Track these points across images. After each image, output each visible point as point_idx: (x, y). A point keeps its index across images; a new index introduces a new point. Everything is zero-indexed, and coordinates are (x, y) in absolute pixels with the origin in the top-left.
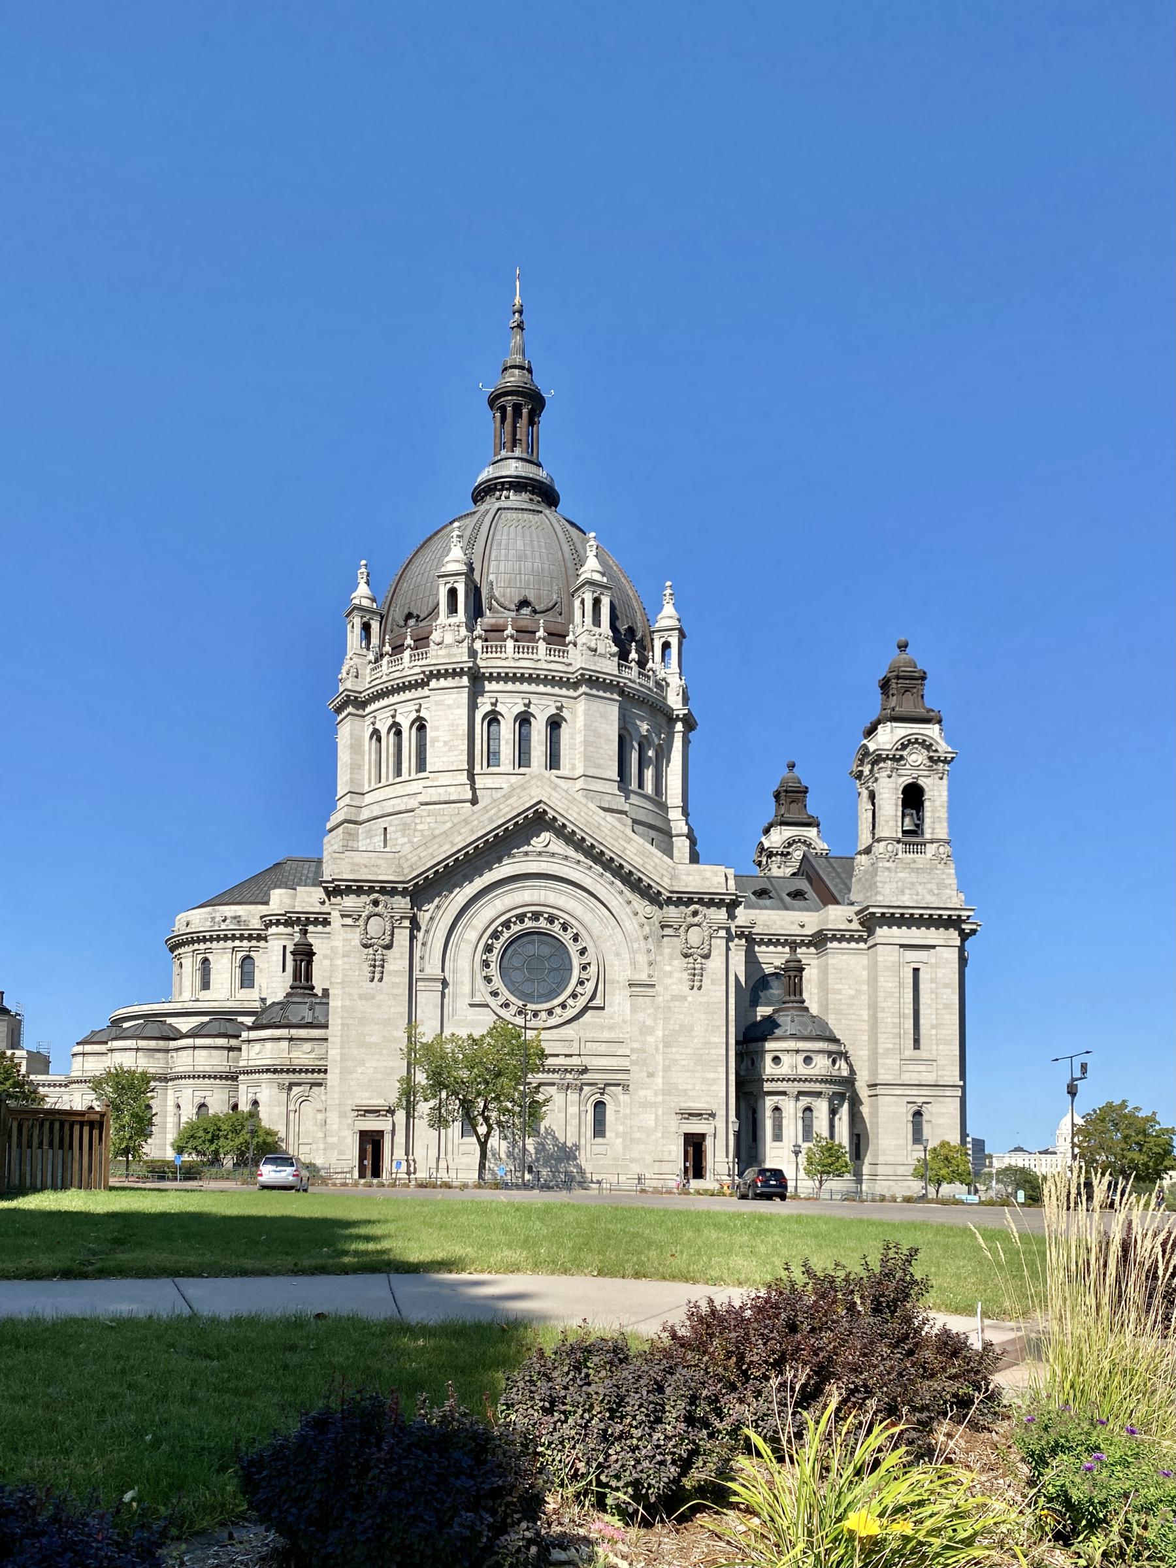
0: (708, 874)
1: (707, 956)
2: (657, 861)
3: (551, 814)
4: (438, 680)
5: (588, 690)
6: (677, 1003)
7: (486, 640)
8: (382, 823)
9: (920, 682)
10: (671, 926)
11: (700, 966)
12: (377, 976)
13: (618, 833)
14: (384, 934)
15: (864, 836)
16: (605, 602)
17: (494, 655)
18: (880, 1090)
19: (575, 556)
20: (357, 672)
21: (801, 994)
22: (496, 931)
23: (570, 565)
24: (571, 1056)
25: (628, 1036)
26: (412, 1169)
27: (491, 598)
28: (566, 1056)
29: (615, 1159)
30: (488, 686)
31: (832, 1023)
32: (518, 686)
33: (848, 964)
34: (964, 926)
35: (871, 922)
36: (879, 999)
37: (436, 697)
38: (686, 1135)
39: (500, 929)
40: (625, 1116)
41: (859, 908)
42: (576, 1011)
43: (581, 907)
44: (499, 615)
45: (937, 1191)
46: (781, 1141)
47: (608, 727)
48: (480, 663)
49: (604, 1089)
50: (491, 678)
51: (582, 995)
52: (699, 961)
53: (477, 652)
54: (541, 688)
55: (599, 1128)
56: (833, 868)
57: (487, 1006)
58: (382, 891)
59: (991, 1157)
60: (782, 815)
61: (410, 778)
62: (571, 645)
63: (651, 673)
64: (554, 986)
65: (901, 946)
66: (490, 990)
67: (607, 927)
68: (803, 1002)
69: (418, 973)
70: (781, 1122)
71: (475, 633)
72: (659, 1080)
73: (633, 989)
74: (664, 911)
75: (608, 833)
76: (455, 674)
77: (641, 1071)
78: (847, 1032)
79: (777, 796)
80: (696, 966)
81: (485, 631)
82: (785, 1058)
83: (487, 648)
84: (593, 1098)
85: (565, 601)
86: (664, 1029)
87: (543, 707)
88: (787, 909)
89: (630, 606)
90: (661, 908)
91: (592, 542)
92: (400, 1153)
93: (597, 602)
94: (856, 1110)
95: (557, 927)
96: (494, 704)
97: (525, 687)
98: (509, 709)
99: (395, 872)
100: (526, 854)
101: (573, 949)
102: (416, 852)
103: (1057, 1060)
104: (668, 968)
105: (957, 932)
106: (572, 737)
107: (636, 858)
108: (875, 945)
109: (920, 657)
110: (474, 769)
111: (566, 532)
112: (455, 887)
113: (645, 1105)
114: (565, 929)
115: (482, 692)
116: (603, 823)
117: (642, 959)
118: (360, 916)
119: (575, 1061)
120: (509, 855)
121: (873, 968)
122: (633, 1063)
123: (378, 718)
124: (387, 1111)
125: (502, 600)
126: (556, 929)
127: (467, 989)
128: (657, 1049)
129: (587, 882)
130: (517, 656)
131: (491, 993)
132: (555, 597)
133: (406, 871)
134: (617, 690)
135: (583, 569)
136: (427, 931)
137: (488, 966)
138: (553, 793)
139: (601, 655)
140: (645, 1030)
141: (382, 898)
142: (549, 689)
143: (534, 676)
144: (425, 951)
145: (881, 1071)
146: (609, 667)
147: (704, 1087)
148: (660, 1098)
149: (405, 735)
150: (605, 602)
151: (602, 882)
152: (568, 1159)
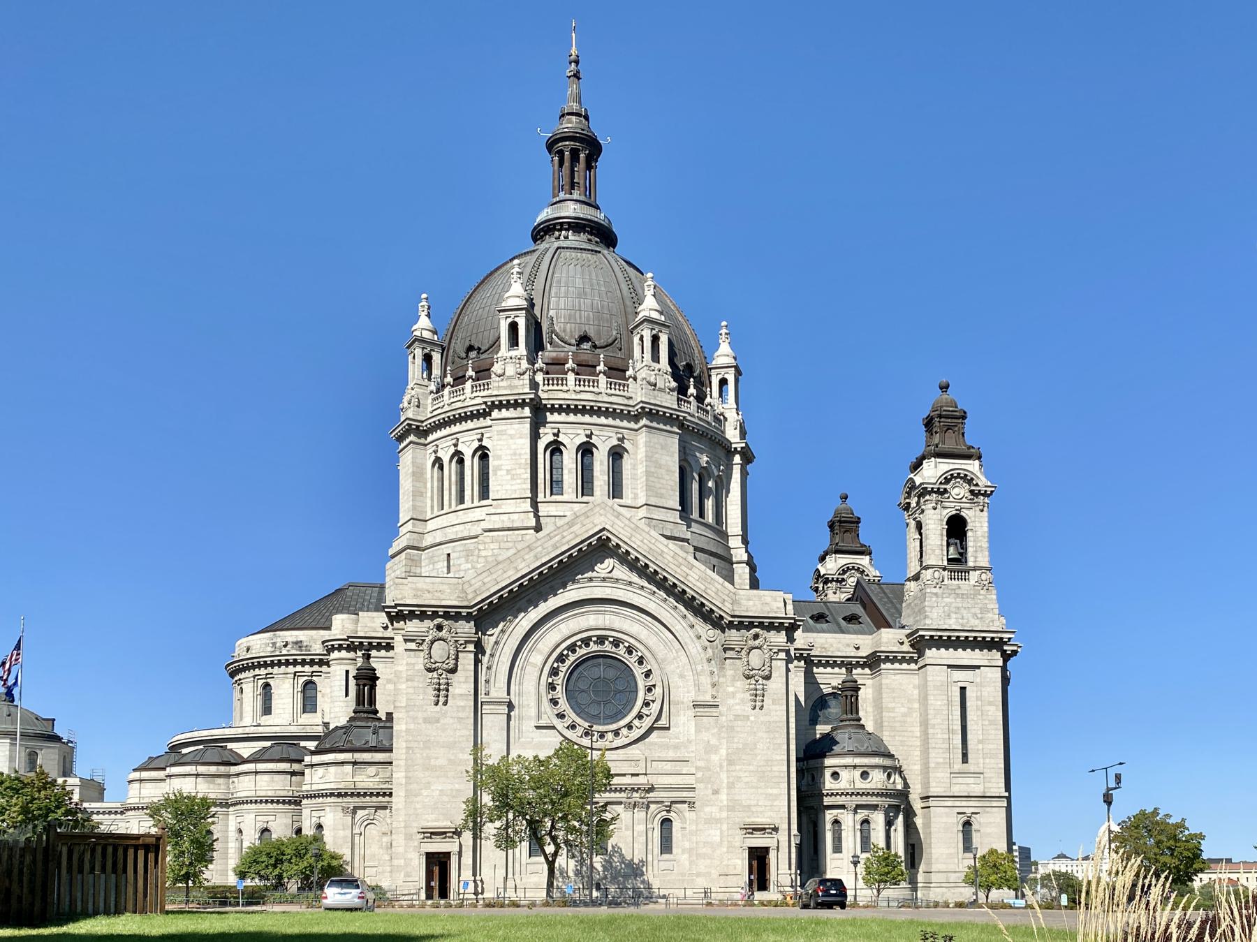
1: (768, 678)
3: (614, 541)
4: (500, 410)
5: (648, 423)
7: (547, 373)
8: (446, 549)
10: (733, 649)
11: (761, 686)
12: (442, 700)
14: (448, 658)
15: (913, 564)
16: (664, 339)
17: (555, 387)
18: (931, 802)
19: (634, 295)
21: (857, 713)
22: (561, 654)
23: (629, 303)
24: (637, 775)
25: (693, 755)
26: (480, 890)
27: (552, 332)
28: (633, 775)
29: (683, 875)
30: (550, 417)
31: (886, 740)
32: (579, 418)
33: (901, 684)
34: (1005, 648)
35: (920, 644)
36: (930, 717)
37: (498, 427)
38: (751, 849)
39: (565, 652)
41: (909, 631)
42: (642, 731)
44: (560, 349)
45: (987, 897)
47: (668, 458)
48: (542, 395)
49: (670, 806)
50: (553, 410)
51: (647, 716)
52: (760, 682)
53: (538, 384)
54: (603, 420)
55: (666, 845)
56: (885, 593)
57: (554, 728)
58: (447, 616)
59: (1036, 863)
60: (837, 544)
61: (473, 506)
62: (631, 380)
63: (709, 408)
64: (620, 707)
65: (949, 666)
66: (556, 713)
67: (672, 651)
68: (859, 720)
69: (483, 696)
70: (841, 834)
71: (536, 365)
72: (723, 797)
74: (726, 634)
76: (516, 405)
77: (706, 788)
78: (901, 748)
79: (831, 526)
80: (758, 687)
81: (547, 364)
82: (844, 774)
83: (548, 381)
84: (659, 816)
85: (624, 338)
86: (728, 748)
87: (605, 438)
88: (843, 632)
89: (688, 344)
90: (723, 632)
91: (650, 282)
92: (467, 874)
93: (655, 339)
94: (910, 822)
95: (621, 651)
96: (557, 435)
97: (587, 419)
98: (572, 439)
99: (459, 597)
100: (591, 579)
101: (638, 672)
102: (480, 577)
103: (1093, 771)
104: (731, 689)
105: (999, 653)
106: (634, 467)
108: (925, 665)
110: (537, 497)
111: (624, 271)
112: (520, 611)
113: (711, 821)
114: (630, 653)
115: (544, 423)
117: (706, 680)
118: (424, 640)
119: (641, 780)
120: (574, 581)
121: (923, 688)
124: (454, 833)
125: (563, 335)
126: (622, 653)
127: (533, 712)
128: (721, 766)
129: (651, 607)
130: (578, 388)
131: (557, 715)
132: (614, 333)
133: (470, 597)
135: (641, 308)
136: (492, 655)
137: (554, 689)
140: (710, 749)
141: (445, 623)
142: (610, 421)
143: (595, 408)
144: (490, 675)
145: (933, 784)
146: (668, 401)
147: (769, 803)
148: (724, 814)
149: (468, 463)
150: (664, 339)
151: (666, 607)
152: (636, 876)
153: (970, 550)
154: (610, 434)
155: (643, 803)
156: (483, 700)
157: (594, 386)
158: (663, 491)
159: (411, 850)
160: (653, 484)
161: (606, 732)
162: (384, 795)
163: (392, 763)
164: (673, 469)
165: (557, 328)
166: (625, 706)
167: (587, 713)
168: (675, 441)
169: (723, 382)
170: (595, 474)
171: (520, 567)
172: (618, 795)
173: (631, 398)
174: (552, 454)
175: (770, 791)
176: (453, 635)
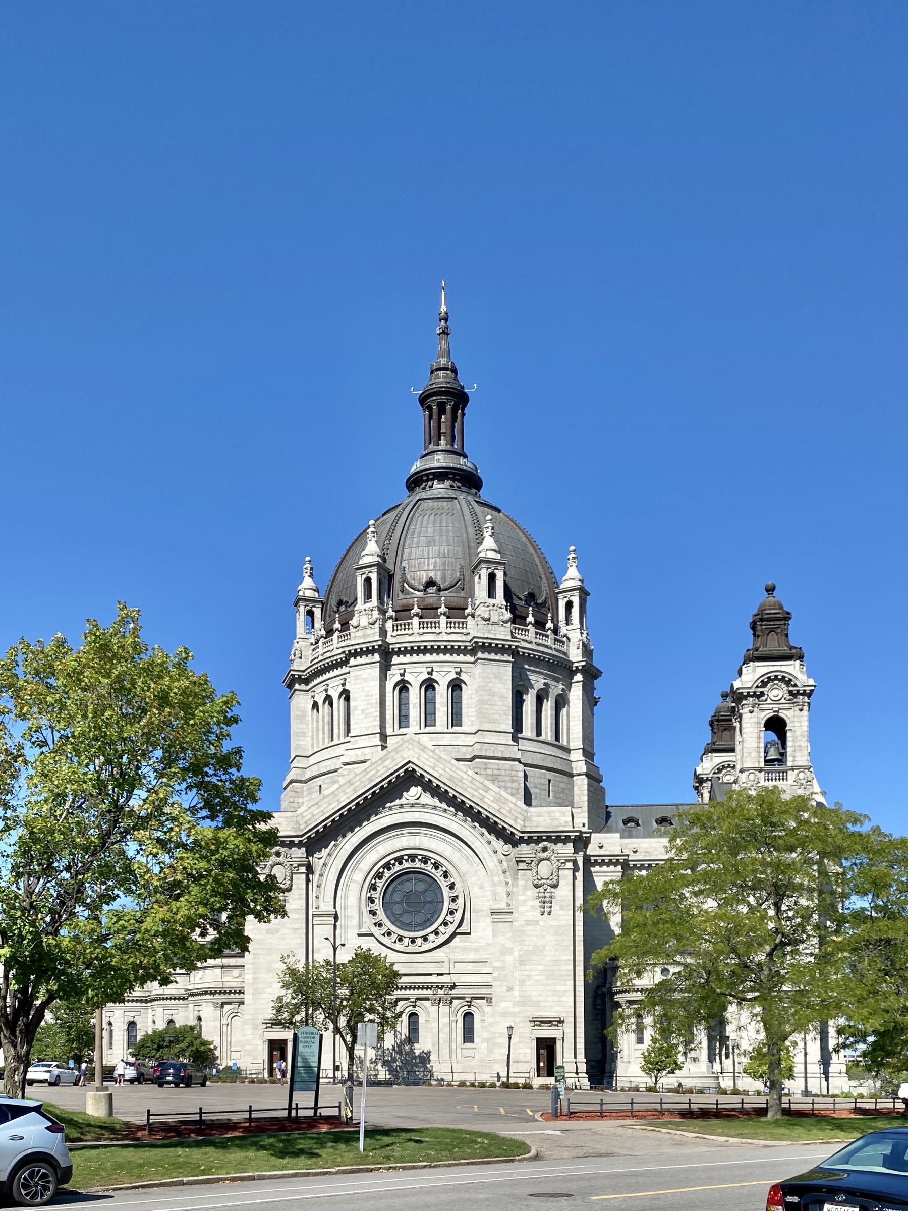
0: (557, 815)
1: (555, 886)
2: (512, 806)
3: (419, 772)
6: (530, 928)
9: (782, 622)
10: (524, 861)
11: (549, 894)
13: (478, 784)
17: (403, 632)
20: (301, 654)
24: (442, 975)
27: (404, 581)
28: (438, 975)
32: (421, 658)
39: (381, 870)
40: (491, 1025)
42: (447, 936)
43: (450, 849)
46: (643, 1043)
47: (501, 686)
49: (471, 1002)
50: (399, 652)
52: (548, 890)
54: (442, 657)
55: (469, 1035)
57: (372, 935)
69: (314, 910)
71: (387, 614)
73: (494, 916)
75: (469, 784)
77: (501, 986)
80: (547, 895)
84: (462, 1009)
87: (443, 674)
97: (428, 657)
99: (293, 828)
101: (444, 884)
102: (310, 811)
104: (521, 898)
107: (494, 805)
109: (785, 598)
114: (437, 868)
116: (465, 776)
117: (502, 890)
118: (266, 865)
119: (445, 979)
122: (495, 979)
123: (330, 686)
126: (429, 869)
127: (355, 922)
130: (422, 631)
131: (375, 924)
134: (511, 652)
136: (321, 875)
137: (373, 902)
138: (423, 754)
139: (493, 623)
140: (505, 951)
141: (282, 850)
142: (448, 657)
146: (502, 633)
151: (467, 826)
153: (789, 750)
154: (450, 669)
155: (447, 999)
156: (314, 913)
157: (435, 627)
158: (497, 717)
159: (258, 1037)
160: (486, 711)
161: (416, 938)
162: (240, 992)
163: (244, 966)
164: (506, 695)
165: (408, 577)
166: (432, 915)
167: (402, 922)
168: (508, 669)
169: (569, 605)
170: (437, 707)
171: (342, 799)
172: (425, 991)
173: (469, 634)
174: (400, 691)
175: (558, 988)
176: (289, 860)
